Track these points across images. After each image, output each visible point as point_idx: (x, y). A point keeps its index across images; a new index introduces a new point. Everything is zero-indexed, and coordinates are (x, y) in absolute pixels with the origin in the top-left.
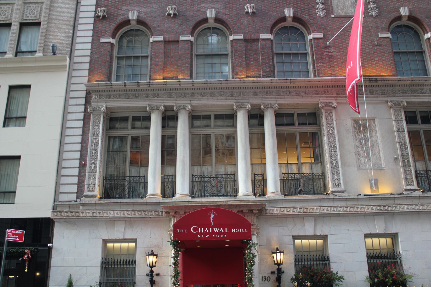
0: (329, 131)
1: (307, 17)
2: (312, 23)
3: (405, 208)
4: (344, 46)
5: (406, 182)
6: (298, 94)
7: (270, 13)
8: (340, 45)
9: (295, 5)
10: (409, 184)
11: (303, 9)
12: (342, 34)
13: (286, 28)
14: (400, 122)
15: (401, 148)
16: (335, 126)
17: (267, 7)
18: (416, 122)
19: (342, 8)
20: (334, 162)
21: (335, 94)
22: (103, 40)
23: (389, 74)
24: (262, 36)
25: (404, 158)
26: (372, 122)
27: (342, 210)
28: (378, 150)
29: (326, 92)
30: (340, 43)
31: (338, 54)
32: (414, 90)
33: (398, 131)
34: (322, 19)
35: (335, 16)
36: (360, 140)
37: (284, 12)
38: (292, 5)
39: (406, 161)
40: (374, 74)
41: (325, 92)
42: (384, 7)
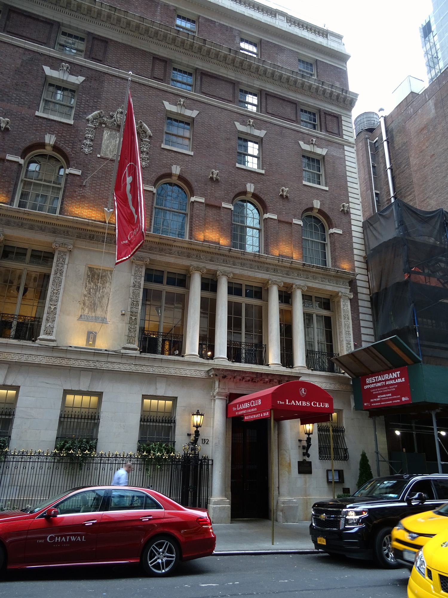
0: (56, 273)
1: (69, 150)
2: (73, 158)
3: (116, 367)
4: (101, 189)
5: (128, 340)
6: (31, 228)
7: (27, 134)
8: (97, 187)
9: (60, 133)
10: (130, 343)
11: (67, 141)
12: (104, 177)
14: (138, 278)
15: (132, 304)
16: (65, 270)
17: (25, 128)
18: (161, 282)
19: (112, 150)
20: (53, 307)
21: (75, 236)
24: (9, 157)
25: (132, 316)
26: (109, 273)
27: (44, 361)
28: (107, 303)
29: (66, 232)
30: (98, 186)
31: (92, 196)
32: (162, 249)
33: (134, 286)
34: (86, 156)
35: (101, 156)
36: (90, 290)
37: (44, 138)
38: (57, 133)
39: (133, 318)
41: (64, 232)
42: (157, 161)
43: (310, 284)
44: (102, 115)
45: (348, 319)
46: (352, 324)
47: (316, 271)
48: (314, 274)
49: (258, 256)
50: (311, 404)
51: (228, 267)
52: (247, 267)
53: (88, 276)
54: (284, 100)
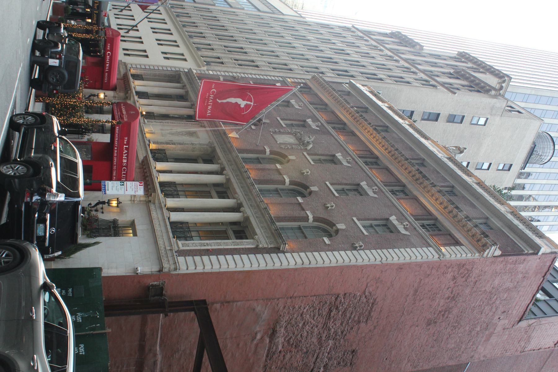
22: (220, 77)
43: (252, 219)
45: (234, 245)
46: (231, 249)
49: (252, 184)
54: (425, 209)
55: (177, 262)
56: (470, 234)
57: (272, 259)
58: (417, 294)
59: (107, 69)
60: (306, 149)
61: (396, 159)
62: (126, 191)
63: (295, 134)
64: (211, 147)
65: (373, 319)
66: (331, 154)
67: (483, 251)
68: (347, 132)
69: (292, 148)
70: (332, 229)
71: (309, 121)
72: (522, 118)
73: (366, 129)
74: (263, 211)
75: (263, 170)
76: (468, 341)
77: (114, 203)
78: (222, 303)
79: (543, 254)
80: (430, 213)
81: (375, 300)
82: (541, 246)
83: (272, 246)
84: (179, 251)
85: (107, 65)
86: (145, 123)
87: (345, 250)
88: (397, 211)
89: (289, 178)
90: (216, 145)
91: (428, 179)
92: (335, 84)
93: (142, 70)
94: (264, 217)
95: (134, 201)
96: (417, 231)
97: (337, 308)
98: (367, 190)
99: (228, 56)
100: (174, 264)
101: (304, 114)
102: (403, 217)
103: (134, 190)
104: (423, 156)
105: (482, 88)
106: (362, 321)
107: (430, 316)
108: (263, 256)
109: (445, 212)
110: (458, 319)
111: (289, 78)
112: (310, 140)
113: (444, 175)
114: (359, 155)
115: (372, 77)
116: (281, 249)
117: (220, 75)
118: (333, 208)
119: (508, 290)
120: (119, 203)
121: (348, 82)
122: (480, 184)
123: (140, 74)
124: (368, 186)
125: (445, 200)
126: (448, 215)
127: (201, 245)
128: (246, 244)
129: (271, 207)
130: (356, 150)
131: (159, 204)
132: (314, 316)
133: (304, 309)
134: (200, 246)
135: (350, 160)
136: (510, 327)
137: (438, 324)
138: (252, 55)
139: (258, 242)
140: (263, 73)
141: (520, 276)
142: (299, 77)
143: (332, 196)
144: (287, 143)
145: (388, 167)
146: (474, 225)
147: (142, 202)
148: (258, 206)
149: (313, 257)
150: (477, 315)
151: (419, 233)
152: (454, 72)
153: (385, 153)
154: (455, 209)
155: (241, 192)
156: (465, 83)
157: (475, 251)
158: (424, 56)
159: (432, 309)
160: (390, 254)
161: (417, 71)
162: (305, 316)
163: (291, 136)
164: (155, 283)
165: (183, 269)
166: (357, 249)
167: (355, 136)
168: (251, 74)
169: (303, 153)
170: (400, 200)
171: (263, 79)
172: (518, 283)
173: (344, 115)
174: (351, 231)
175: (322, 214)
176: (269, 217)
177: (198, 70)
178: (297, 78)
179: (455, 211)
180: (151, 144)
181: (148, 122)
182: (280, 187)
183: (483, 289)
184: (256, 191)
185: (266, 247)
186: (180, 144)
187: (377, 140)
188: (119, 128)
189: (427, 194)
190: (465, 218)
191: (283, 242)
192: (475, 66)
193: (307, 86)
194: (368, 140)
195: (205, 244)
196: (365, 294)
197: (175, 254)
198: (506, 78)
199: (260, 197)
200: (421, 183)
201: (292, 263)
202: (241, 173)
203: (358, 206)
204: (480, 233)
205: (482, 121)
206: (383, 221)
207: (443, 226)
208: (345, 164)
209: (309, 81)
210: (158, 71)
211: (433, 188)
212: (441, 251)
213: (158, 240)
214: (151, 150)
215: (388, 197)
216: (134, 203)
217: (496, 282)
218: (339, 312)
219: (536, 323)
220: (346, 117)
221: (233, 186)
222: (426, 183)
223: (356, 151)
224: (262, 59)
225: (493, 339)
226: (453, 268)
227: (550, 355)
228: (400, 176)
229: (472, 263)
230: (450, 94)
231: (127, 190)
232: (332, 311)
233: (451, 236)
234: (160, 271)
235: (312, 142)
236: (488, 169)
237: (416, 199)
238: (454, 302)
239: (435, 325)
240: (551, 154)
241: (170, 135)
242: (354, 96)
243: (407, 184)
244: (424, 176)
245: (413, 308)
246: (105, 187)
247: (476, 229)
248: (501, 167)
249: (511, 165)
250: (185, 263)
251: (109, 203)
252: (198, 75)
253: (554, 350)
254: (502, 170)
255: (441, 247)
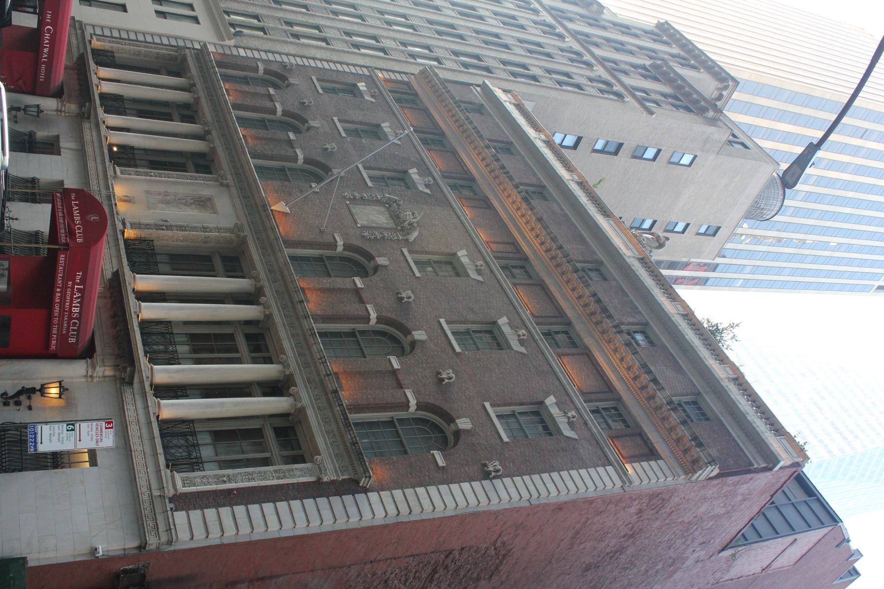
13: (441, 431)
22: (259, 64)
23: (283, 234)
27: (91, 164)
33: (204, 228)
40: (278, 222)
43: (311, 414)
44: (398, 203)
45: (278, 478)
46: (272, 486)
47: (335, 411)
48: (331, 418)
49: (313, 332)
50: (79, 224)
51: (279, 311)
52: (290, 330)
53: (200, 198)
54: (602, 377)
55: (172, 527)
56: (674, 437)
57: (345, 507)
58: (578, 536)
59: (45, 58)
60: (407, 240)
61: (558, 266)
62: (78, 441)
63: (387, 204)
64: (238, 236)
65: (501, 573)
66: (447, 250)
67: (693, 471)
68: (478, 200)
69: (383, 238)
70: (449, 425)
71: (413, 171)
72: (749, 159)
73: (509, 196)
74: (330, 396)
75: (332, 291)
76: (640, 582)
77: (54, 391)
78: (251, 581)
79: (781, 468)
80: (609, 387)
81: (510, 551)
82: (780, 459)
83: (345, 477)
84: (177, 496)
85: (46, 50)
86: (115, 177)
87: (470, 480)
88: (557, 383)
89: (377, 311)
90: (247, 233)
91: (610, 317)
92: (459, 87)
93: (113, 42)
94: (331, 407)
95: (91, 376)
96: (590, 430)
97: (447, 566)
98: (508, 337)
99: (273, 14)
100: (167, 531)
101: (404, 156)
102: (567, 398)
103: (95, 438)
104: (601, 255)
105: (695, 102)
106: (482, 578)
107: (591, 560)
108: (329, 501)
109: (635, 386)
110: (633, 559)
111: (381, 70)
112: (415, 220)
113: (634, 300)
114: (496, 254)
115: (520, 72)
116: (361, 485)
117: (258, 60)
118: (452, 381)
119: (717, 517)
120: (63, 390)
121: (480, 83)
122: (689, 316)
123: (110, 49)
124: (511, 327)
125: (638, 363)
126: (639, 392)
127: (219, 480)
128: (300, 474)
129: (344, 381)
130: (491, 242)
131: (140, 383)
132: (406, 580)
133: (392, 574)
134: (216, 483)
135: (481, 266)
136: (706, 558)
137: (601, 568)
138: (317, 14)
139: (320, 470)
140: (335, 58)
141: (740, 498)
142: (397, 69)
143: (451, 352)
144: (374, 225)
145: (543, 281)
146: (681, 419)
147: (106, 379)
148: (322, 383)
149: (416, 499)
150: (662, 551)
151: (592, 434)
152: (651, 65)
153: (541, 250)
154: (651, 384)
155: (292, 348)
156: (667, 90)
157: (680, 472)
158: (604, 28)
159: (596, 552)
160: (545, 484)
161: (593, 61)
162: (391, 582)
163: (382, 209)
164: (131, 567)
165: (183, 540)
166: (491, 476)
167: (490, 208)
168: (314, 59)
169: (402, 251)
170: (562, 357)
171: (335, 71)
172: (733, 507)
173: (474, 162)
174: (481, 433)
175: (434, 399)
176: (341, 410)
177: (220, 44)
178: (393, 72)
179: (651, 384)
180: (126, 230)
181: (122, 173)
182: (361, 326)
183: (680, 520)
184: (320, 350)
185: (335, 478)
186: (181, 228)
187: (527, 223)
188: (66, 258)
189: (607, 345)
190: (668, 404)
191: (365, 473)
192: (682, 53)
193: (410, 89)
194: (511, 218)
195: (225, 479)
196: (495, 546)
197: (169, 506)
198: (731, 83)
199: (325, 364)
200: (598, 323)
201: (380, 513)
202: (292, 302)
203: (494, 375)
204: (690, 438)
205: (687, 159)
206: (535, 406)
207: (629, 413)
208: (473, 275)
209: (415, 77)
210: (145, 47)
211: (617, 334)
212: (625, 472)
213: (137, 476)
214: (126, 241)
215: (543, 353)
216: (92, 381)
217: (702, 509)
218: (449, 571)
219: (744, 550)
220: (476, 167)
221: (277, 331)
222: (607, 323)
223: (492, 245)
224: (335, 25)
225: (677, 576)
226: (641, 499)
227: (752, 583)
228: (563, 303)
229: (672, 491)
230: (645, 115)
231: (80, 440)
232: (436, 572)
233: (642, 438)
234: (142, 547)
235: (418, 222)
236: (683, 232)
237: (587, 355)
238: (631, 540)
239: (596, 571)
240: (777, 208)
241: (164, 206)
242: (490, 115)
243: (574, 322)
244: (605, 310)
245: (566, 554)
246: (35, 438)
247: (683, 428)
248: (702, 230)
249: (719, 228)
250: (187, 526)
251: (42, 390)
252: (218, 58)
253: (759, 576)
254: (704, 234)
255: (627, 463)
